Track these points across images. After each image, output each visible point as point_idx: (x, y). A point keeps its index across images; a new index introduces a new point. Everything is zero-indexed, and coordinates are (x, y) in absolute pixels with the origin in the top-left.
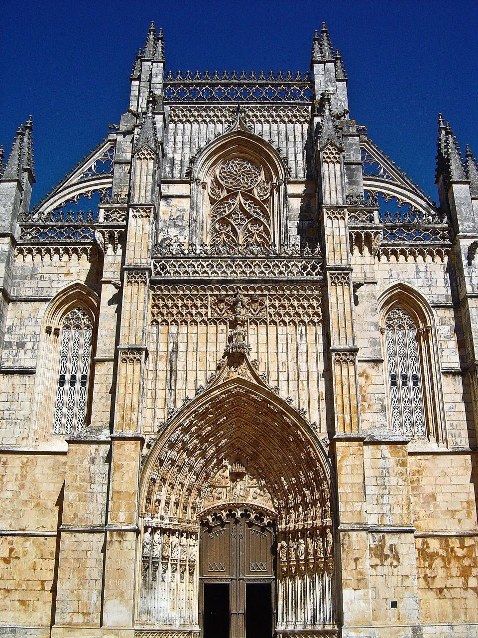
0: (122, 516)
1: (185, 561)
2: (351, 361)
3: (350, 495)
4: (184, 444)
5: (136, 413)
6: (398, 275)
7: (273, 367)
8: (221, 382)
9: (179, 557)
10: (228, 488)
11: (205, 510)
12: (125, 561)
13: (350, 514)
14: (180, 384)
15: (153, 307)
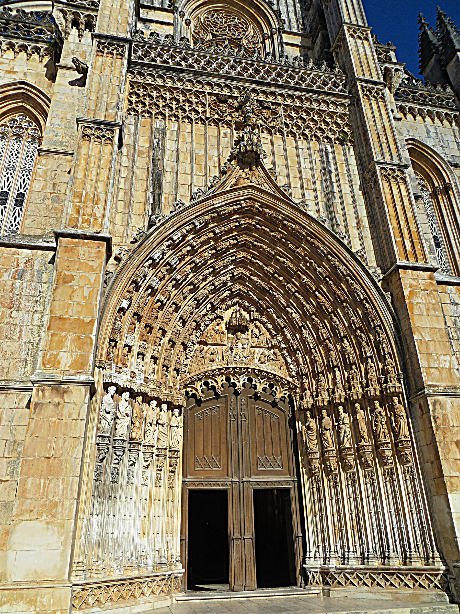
0: (66, 359)
1: (166, 449)
2: (402, 178)
3: (431, 345)
4: (172, 270)
5: (101, 206)
6: (408, 131)
7: (295, 183)
8: (228, 188)
9: (155, 442)
10: (224, 348)
11: (191, 375)
12: (65, 441)
13: (437, 372)
14: (166, 188)
15: (130, 94)
